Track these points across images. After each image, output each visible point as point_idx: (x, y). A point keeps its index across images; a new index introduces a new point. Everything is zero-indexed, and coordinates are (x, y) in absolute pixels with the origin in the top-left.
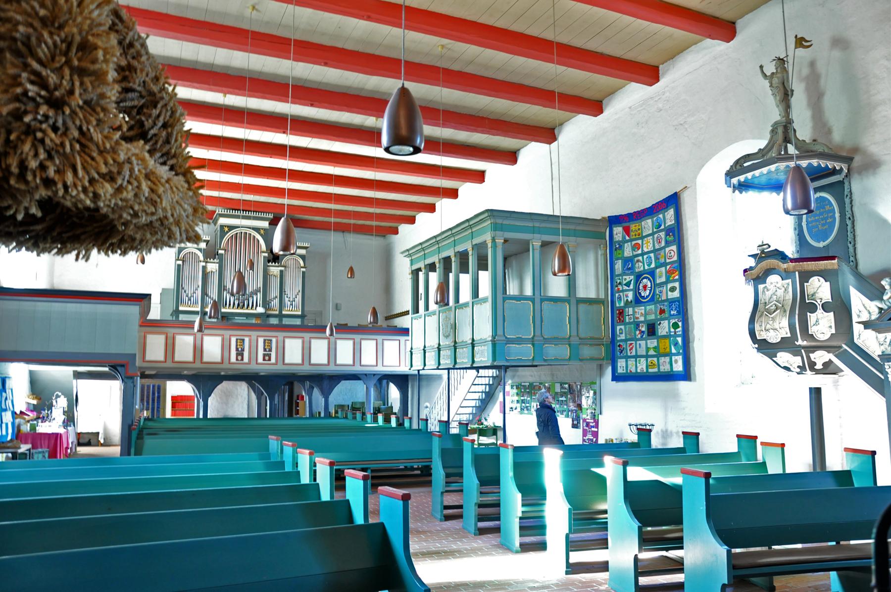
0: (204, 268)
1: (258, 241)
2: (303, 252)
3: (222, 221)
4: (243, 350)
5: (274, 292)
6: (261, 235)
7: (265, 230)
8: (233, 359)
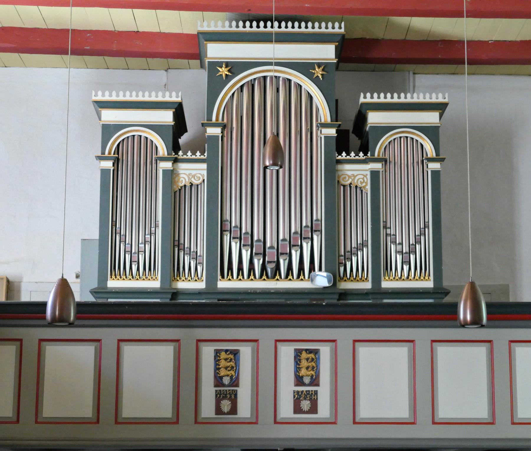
0: (170, 176)
1: (310, 98)
2: (431, 118)
3: (215, 51)
4: (235, 382)
5: (359, 232)
6: (316, 81)
7: (325, 66)
8: (208, 410)
